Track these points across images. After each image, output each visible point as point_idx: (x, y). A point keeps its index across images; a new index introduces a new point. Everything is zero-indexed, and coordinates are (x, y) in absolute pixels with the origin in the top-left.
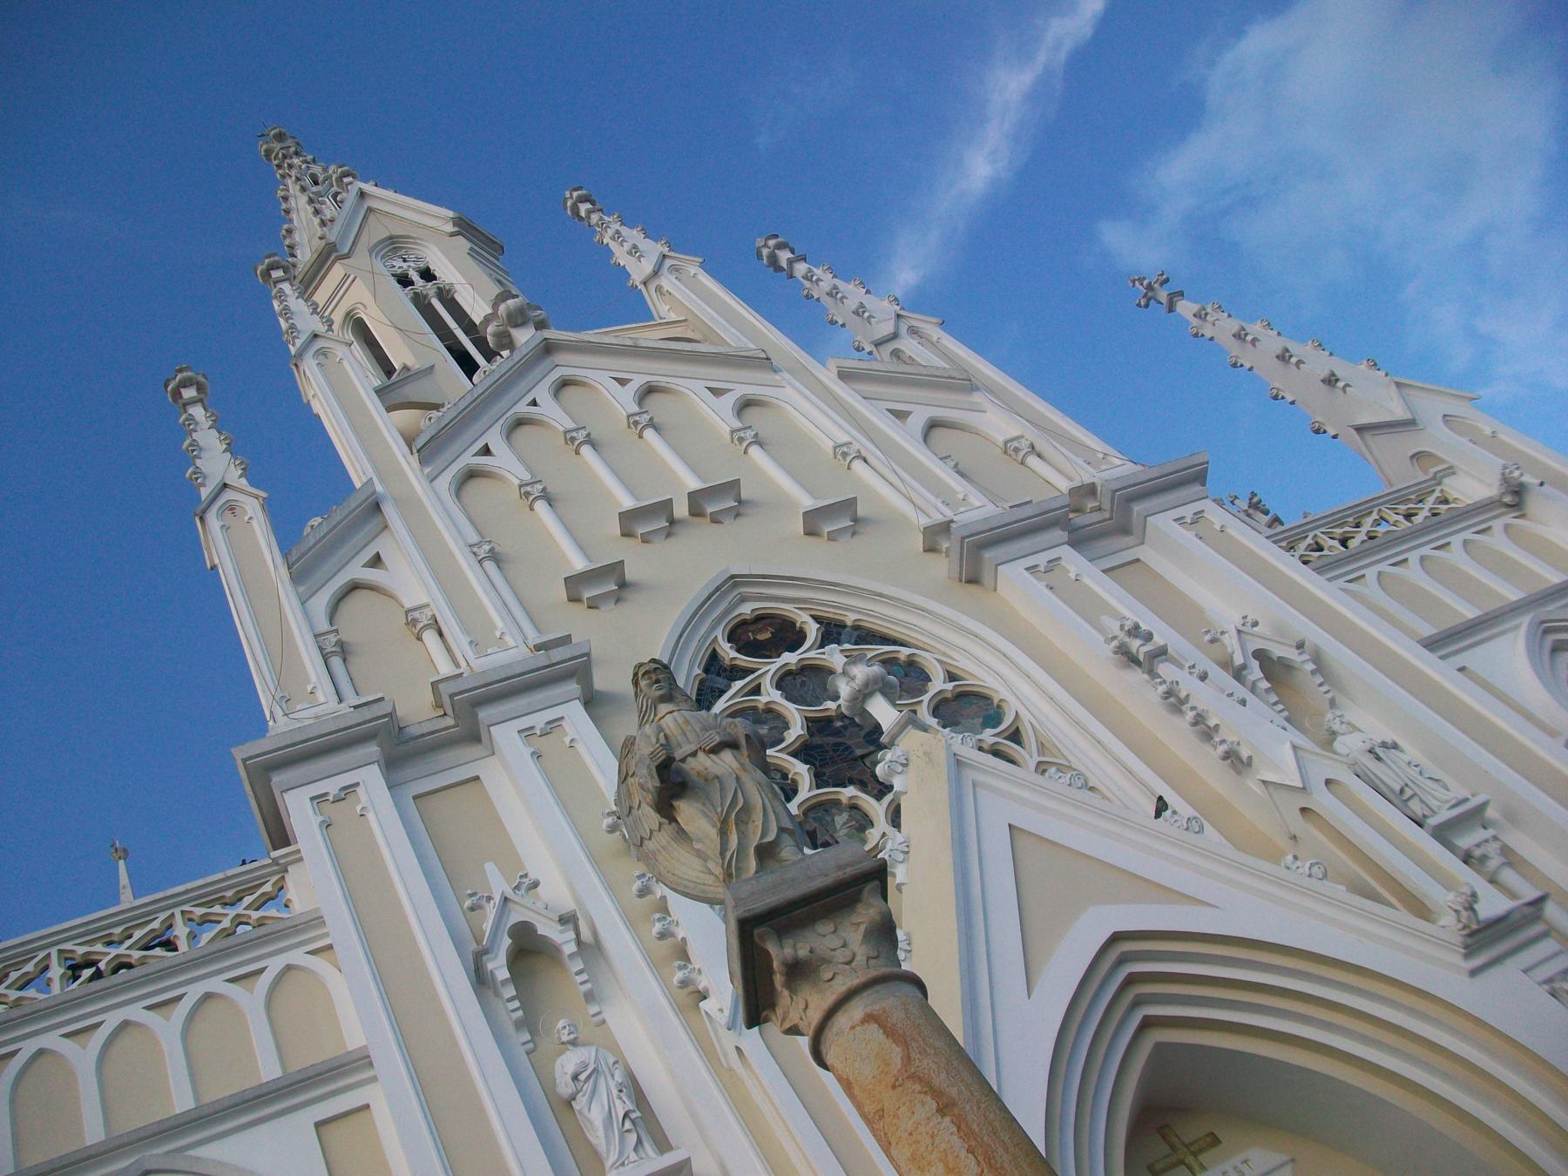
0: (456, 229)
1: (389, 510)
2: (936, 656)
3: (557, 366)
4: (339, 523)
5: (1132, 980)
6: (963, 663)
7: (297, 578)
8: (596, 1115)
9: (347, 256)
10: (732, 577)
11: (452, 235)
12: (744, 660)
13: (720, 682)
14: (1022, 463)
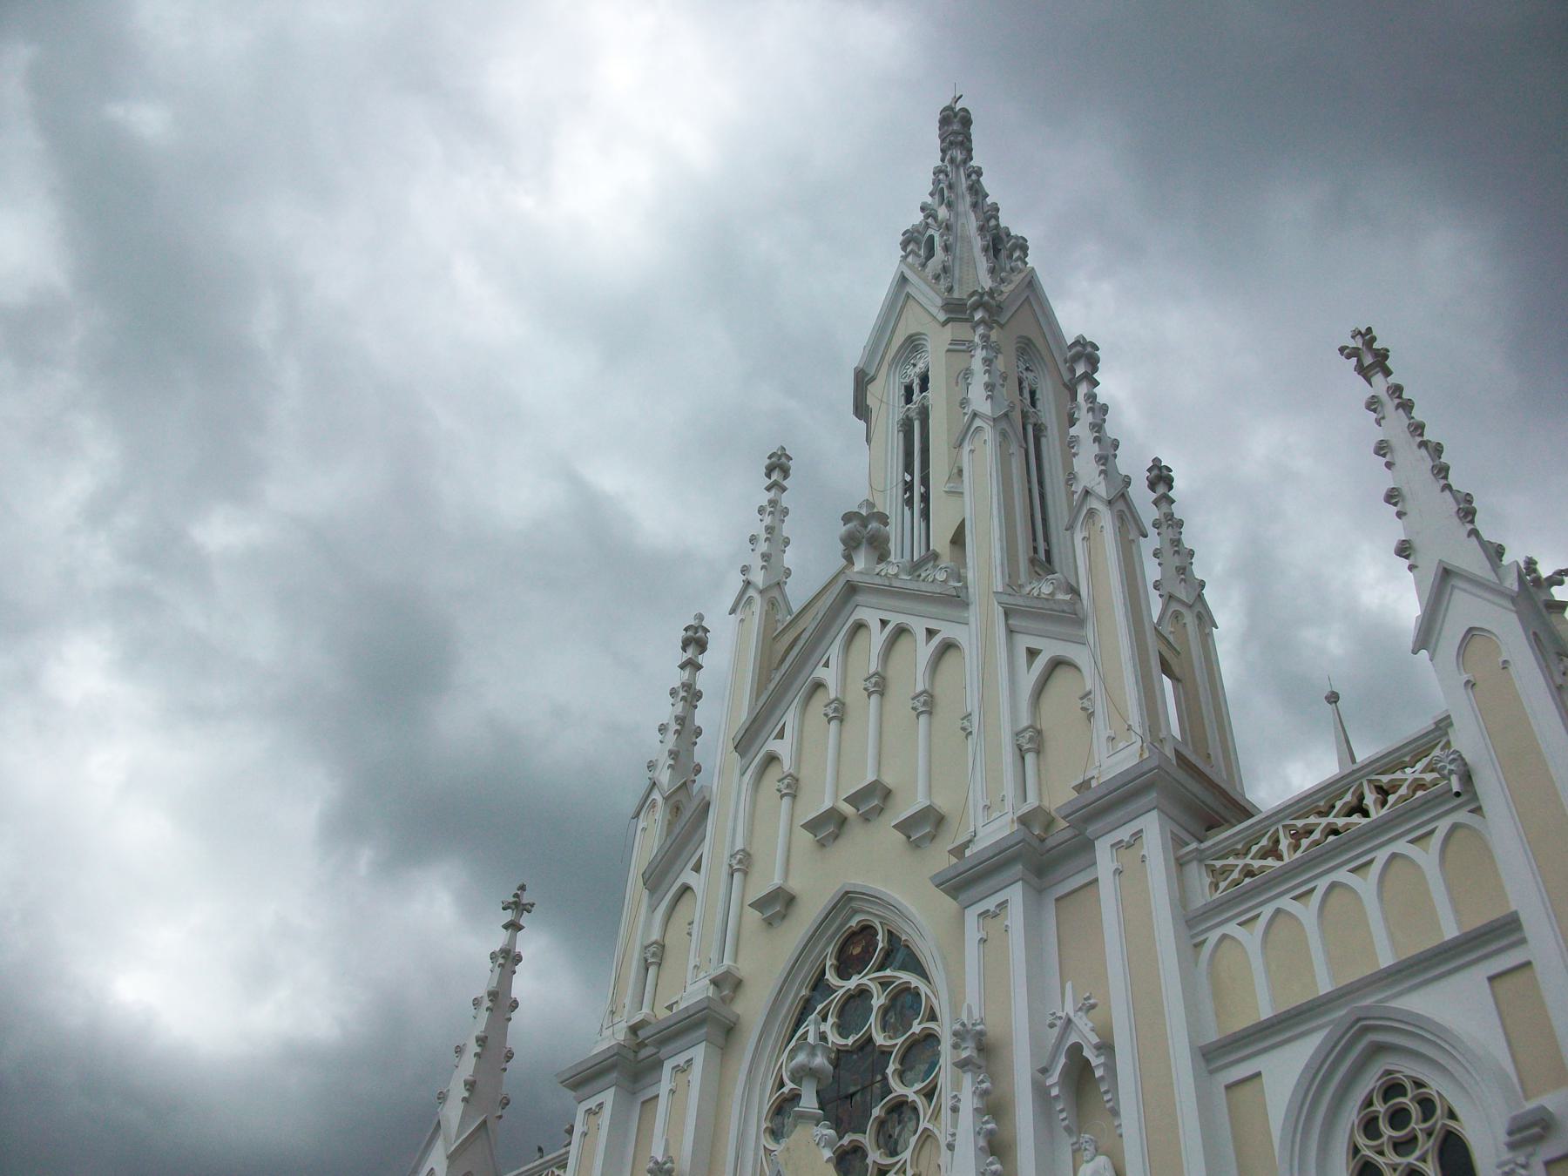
0: (948, 316)
3: (857, 605)
4: (679, 834)
10: (847, 893)
11: (944, 324)
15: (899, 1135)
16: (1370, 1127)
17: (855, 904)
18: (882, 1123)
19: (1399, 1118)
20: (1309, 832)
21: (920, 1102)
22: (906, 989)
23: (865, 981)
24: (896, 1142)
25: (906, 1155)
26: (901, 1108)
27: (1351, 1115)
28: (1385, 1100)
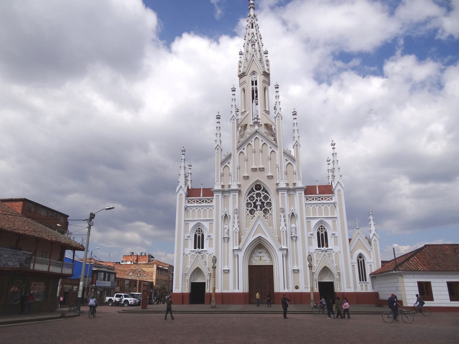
1: (232, 156)
5: (260, 239)
6: (271, 199)
7: (221, 164)
8: (225, 231)
9: (246, 75)
11: (262, 75)
14: (294, 174)
16: (319, 229)
17: (259, 182)
18: (263, 210)
19: (322, 229)
20: (317, 199)
22: (266, 195)
23: (260, 192)
24: (266, 213)
25: (268, 215)
26: (266, 209)
27: (318, 227)
28: (324, 228)
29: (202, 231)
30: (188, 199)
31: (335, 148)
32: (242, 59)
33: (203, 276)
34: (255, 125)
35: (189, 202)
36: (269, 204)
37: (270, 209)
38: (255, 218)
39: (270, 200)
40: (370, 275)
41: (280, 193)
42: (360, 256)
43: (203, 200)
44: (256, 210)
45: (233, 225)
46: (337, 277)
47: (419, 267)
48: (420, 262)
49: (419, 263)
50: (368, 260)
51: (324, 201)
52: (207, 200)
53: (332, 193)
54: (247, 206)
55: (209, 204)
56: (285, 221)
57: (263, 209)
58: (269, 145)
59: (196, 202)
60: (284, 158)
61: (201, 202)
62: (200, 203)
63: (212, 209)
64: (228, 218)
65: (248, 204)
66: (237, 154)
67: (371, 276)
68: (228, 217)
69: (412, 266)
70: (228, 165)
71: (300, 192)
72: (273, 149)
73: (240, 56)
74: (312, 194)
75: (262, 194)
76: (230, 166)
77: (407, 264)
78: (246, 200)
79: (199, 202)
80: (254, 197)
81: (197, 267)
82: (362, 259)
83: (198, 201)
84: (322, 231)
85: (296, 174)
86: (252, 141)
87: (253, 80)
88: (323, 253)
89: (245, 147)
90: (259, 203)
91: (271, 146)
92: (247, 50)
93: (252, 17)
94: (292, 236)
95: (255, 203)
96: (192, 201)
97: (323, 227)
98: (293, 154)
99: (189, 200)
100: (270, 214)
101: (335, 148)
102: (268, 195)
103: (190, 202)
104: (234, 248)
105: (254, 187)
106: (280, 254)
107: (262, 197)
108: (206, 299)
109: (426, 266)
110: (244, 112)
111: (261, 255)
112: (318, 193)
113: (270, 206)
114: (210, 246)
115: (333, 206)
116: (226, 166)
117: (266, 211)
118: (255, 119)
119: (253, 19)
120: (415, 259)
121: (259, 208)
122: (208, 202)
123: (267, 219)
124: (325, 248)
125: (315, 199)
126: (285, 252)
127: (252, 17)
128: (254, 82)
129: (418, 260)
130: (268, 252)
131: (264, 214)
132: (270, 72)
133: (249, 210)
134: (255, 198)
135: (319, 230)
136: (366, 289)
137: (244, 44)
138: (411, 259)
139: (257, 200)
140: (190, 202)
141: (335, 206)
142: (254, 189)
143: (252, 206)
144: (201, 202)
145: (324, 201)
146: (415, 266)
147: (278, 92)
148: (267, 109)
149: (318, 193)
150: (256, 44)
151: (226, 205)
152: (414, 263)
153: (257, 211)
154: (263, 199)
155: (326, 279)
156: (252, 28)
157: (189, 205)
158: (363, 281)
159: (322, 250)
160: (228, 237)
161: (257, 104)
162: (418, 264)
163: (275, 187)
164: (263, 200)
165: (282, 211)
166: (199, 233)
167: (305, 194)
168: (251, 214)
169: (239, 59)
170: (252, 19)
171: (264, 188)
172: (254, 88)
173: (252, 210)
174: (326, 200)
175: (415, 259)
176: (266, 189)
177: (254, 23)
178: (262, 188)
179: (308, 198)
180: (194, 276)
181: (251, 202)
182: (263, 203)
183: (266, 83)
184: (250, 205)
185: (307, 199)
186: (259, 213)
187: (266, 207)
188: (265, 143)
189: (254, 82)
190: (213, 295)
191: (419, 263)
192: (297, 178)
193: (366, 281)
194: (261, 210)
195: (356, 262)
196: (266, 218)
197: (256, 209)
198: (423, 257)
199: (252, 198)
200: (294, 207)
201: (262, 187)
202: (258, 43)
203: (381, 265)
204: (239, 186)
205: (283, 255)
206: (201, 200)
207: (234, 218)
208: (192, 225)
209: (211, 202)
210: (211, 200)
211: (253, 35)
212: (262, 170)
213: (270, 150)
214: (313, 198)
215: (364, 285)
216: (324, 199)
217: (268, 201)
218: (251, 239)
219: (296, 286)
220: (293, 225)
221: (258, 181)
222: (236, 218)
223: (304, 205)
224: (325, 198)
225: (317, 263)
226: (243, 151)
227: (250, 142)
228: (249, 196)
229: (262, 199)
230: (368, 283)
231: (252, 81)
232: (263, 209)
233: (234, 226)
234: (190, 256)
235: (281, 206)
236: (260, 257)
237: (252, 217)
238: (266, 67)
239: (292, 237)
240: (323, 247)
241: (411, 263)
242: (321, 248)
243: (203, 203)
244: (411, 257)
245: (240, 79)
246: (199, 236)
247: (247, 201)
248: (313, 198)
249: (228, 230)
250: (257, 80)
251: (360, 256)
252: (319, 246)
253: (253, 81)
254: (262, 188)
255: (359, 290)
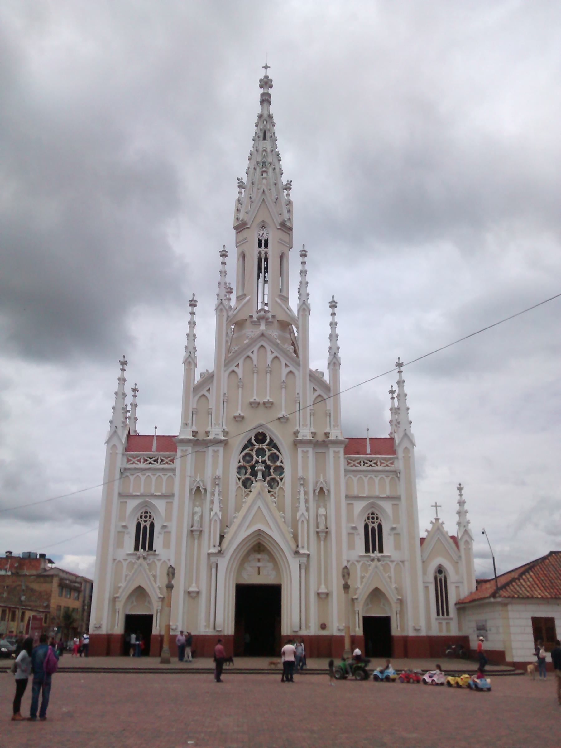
2: (282, 457)
6: (284, 461)
9: (248, 228)
12: (255, 443)
13: (249, 445)
15: (273, 484)
19: (373, 518)
20: (367, 463)
21: (280, 481)
22: (275, 454)
26: (273, 479)
27: (366, 516)
29: (150, 517)
30: (127, 455)
31: (402, 371)
32: (243, 196)
33: (150, 602)
34: (260, 322)
35: (129, 460)
36: (280, 470)
37: (281, 479)
38: (252, 496)
39: (282, 462)
40: (456, 604)
41: (300, 450)
42: (440, 570)
43: (156, 458)
44: (254, 480)
45: (211, 507)
46: (395, 607)
47: (535, 592)
48: (538, 582)
49: (537, 585)
50: (452, 577)
51: (379, 468)
52: (164, 459)
53: (394, 452)
54: (239, 473)
55: (166, 466)
56: (307, 501)
57: (268, 479)
58: (284, 362)
59: (142, 461)
60: (309, 386)
61: (153, 462)
62: (150, 463)
63: (173, 476)
64: (203, 493)
65: (240, 468)
66: (224, 375)
67: (458, 606)
68: (203, 491)
69: (523, 589)
70: (206, 394)
71: (336, 450)
72: (291, 368)
73: (238, 190)
74: (358, 453)
75: (267, 451)
76: (212, 397)
77: (516, 586)
78: (238, 461)
79: (148, 462)
80: (252, 457)
81: (139, 585)
82: (443, 575)
83: (147, 460)
84: (373, 523)
85: (330, 416)
86: (253, 352)
87: (260, 239)
88: (373, 564)
89: (241, 362)
90: (260, 467)
91: (288, 363)
92: (253, 180)
93: (265, 120)
94: (317, 530)
95: (253, 467)
96: (134, 458)
97: (375, 516)
98: (327, 378)
99: (130, 458)
100: (281, 487)
101: (402, 371)
102: (278, 453)
103: (130, 460)
104: (211, 551)
105: (253, 438)
106: (294, 564)
107: (266, 458)
108: (154, 647)
109: (548, 591)
110: (241, 296)
111: (259, 564)
112: (368, 451)
113: (282, 473)
114: (167, 545)
115: (394, 476)
116: (204, 395)
117: (273, 483)
118: (261, 312)
119: (267, 122)
120: (531, 576)
121: (260, 476)
122: (164, 462)
123: (275, 498)
124: (377, 554)
125: (362, 463)
126: (304, 560)
127: (265, 120)
128: (263, 242)
129: (535, 579)
130: (272, 558)
131: (269, 488)
132: (292, 226)
133: (241, 480)
134: (255, 457)
135: (367, 521)
136: (448, 630)
137: (249, 168)
138: (524, 577)
139: (257, 462)
140: (130, 460)
141: (399, 478)
142: (253, 441)
143: (247, 472)
144: (153, 462)
145: (379, 468)
146: (528, 589)
147: (305, 263)
148: (284, 294)
149: (368, 451)
150: (270, 170)
151: (200, 467)
152: (528, 583)
153: (256, 481)
154: (269, 460)
155: (376, 612)
156: (265, 138)
157: (129, 466)
158: (443, 615)
159: (372, 558)
160: (201, 529)
161: (265, 282)
162: (535, 586)
163: (291, 439)
164: (269, 463)
165: (302, 483)
166: (145, 521)
167: (346, 453)
168: (246, 487)
169: (237, 196)
170: (265, 122)
171: (271, 440)
172: (263, 253)
173: (248, 479)
174: (383, 465)
175: (531, 576)
176: (274, 442)
177: (269, 130)
178: (268, 440)
179: (351, 460)
180: (132, 602)
181: (247, 465)
182: (268, 467)
183: (284, 245)
184: (243, 471)
185: (349, 463)
186: (259, 485)
187: (273, 476)
188: (276, 357)
189: (263, 242)
190: (166, 639)
191: (537, 585)
192: (332, 423)
193: (448, 614)
194: (264, 481)
195: (432, 580)
196: (272, 495)
197: (255, 479)
198: (544, 574)
199: (247, 457)
200: (325, 476)
201: (268, 438)
202: (274, 169)
203: (475, 587)
204: (226, 433)
205: (300, 565)
206: (152, 458)
207: (213, 494)
208: (132, 504)
209: (171, 463)
210: (172, 458)
211: (264, 153)
212: (268, 405)
213: (285, 371)
214: (359, 461)
215: (444, 622)
216: (379, 463)
217: (278, 463)
218: (244, 534)
219: (322, 625)
220: (322, 511)
221: (261, 426)
222: (217, 494)
223: (342, 473)
224: (380, 462)
225: (362, 582)
226: (236, 369)
227: (250, 354)
228: (243, 454)
229: (267, 460)
230: (451, 619)
231: (259, 239)
232: (268, 479)
233: (211, 510)
234: (125, 564)
235: (300, 474)
236: (259, 568)
237: (248, 492)
238: (286, 216)
239: (317, 532)
240: (373, 552)
241: (524, 583)
242: (371, 554)
243: (155, 463)
244: (524, 573)
245: (237, 233)
246: (145, 527)
247: (239, 462)
248: (360, 462)
249: (201, 517)
250: (268, 239)
251: (440, 570)
252: (367, 550)
253: (261, 240)
254: (268, 440)
255: (435, 632)
